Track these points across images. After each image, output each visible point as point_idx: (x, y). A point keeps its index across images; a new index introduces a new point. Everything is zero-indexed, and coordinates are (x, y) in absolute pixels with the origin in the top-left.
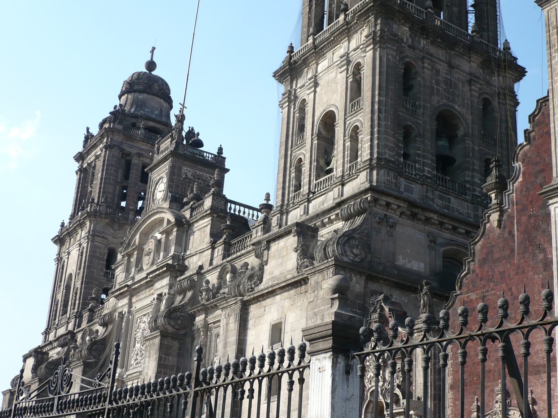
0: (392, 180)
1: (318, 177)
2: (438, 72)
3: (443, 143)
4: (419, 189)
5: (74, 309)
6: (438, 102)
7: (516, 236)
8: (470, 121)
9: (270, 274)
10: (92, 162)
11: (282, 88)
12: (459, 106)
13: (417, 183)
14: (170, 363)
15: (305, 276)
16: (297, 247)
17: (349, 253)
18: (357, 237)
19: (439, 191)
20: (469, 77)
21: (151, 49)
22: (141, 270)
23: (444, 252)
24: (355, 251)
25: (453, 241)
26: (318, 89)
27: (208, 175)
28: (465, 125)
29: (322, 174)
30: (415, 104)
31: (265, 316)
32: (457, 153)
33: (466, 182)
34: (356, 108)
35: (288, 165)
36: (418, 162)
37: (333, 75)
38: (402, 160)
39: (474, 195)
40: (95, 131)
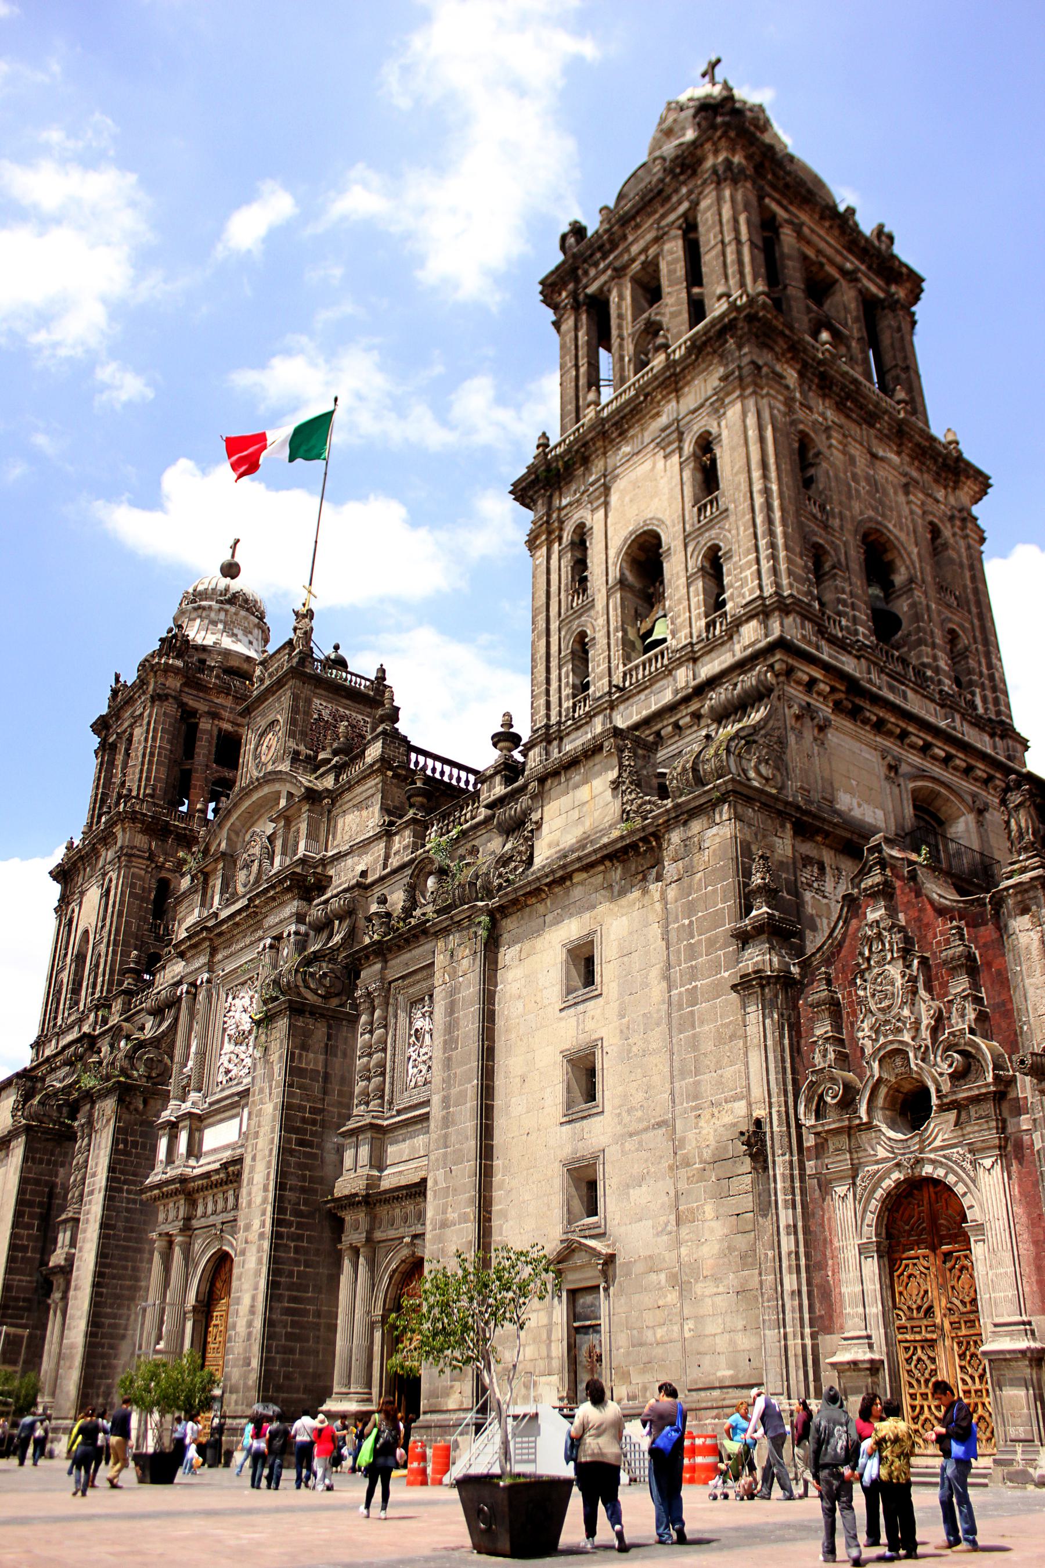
1: (627, 658)
2: (852, 460)
5: (93, 993)
6: (861, 513)
8: (915, 557)
9: (550, 846)
10: (125, 731)
11: (529, 515)
13: (850, 653)
14: (311, 1066)
15: (651, 830)
17: (752, 774)
19: (888, 675)
20: (904, 480)
21: (232, 543)
22: (234, 898)
23: (914, 791)
24: (763, 769)
26: (614, 498)
27: (360, 717)
28: (908, 562)
29: (633, 655)
32: (902, 607)
33: (924, 665)
34: (708, 513)
37: (647, 466)
40: (130, 677)
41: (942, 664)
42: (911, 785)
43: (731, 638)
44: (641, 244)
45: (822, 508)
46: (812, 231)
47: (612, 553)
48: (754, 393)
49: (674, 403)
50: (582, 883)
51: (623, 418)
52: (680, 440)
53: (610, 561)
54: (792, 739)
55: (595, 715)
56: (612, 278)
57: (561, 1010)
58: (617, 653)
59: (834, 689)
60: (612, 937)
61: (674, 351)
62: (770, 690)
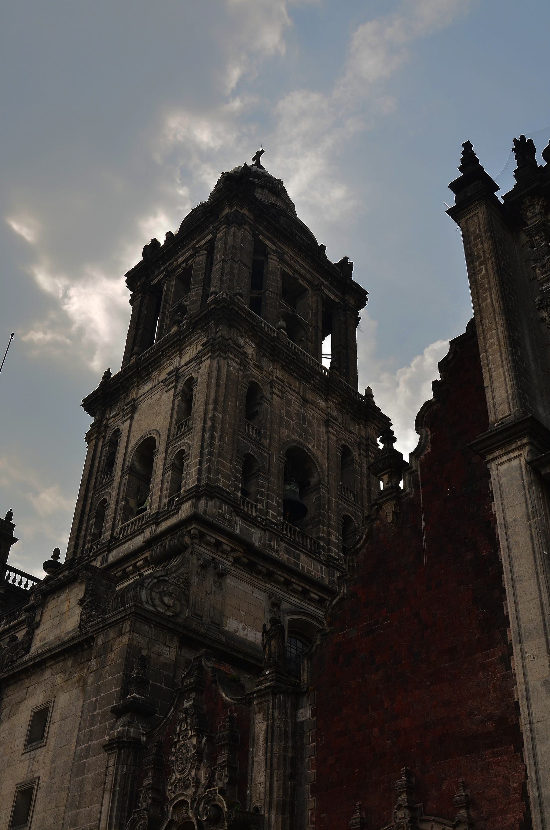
0: (224, 514)
2: (288, 403)
3: (292, 487)
4: (260, 536)
6: (288, 436)
7: (424, 532)
8: (325, 467)
11: (92, 420)
12: (313, 446)
13: (258, 527)
15: (90, 634)
16: (84, 597)
17: (157, 602)
18: (171, 581)
19: (286, 542)
24: (166, 600)
25: (302, 608)
26: (136, 416)
30: (260, 432)
31: (26, 702)
33: (319, 538)
34: (183, 430)
35: (88, 509)
36: (261, 501)
37: (157, 396)
38: (239, 494)
39: (330, 555)
41: (333, 538)
42: (290, 617)
43: (178, 512)
44: (185, 257)
45: (258, 432)
46: (291, 258)
47: (130, 449)
48: (219, 355)
49: (178, 358)
50: (50, 666)
51: (149, 364)
52: (177, 381)
53: (128, 455)
54: (195, 581)
55: (98, 555)
56: (165, 277)
57: (22, 754)
58: (120, 515)
59: (233, 550)
60: (59, 706)
61: (183, 325)
62: (185, 547)
